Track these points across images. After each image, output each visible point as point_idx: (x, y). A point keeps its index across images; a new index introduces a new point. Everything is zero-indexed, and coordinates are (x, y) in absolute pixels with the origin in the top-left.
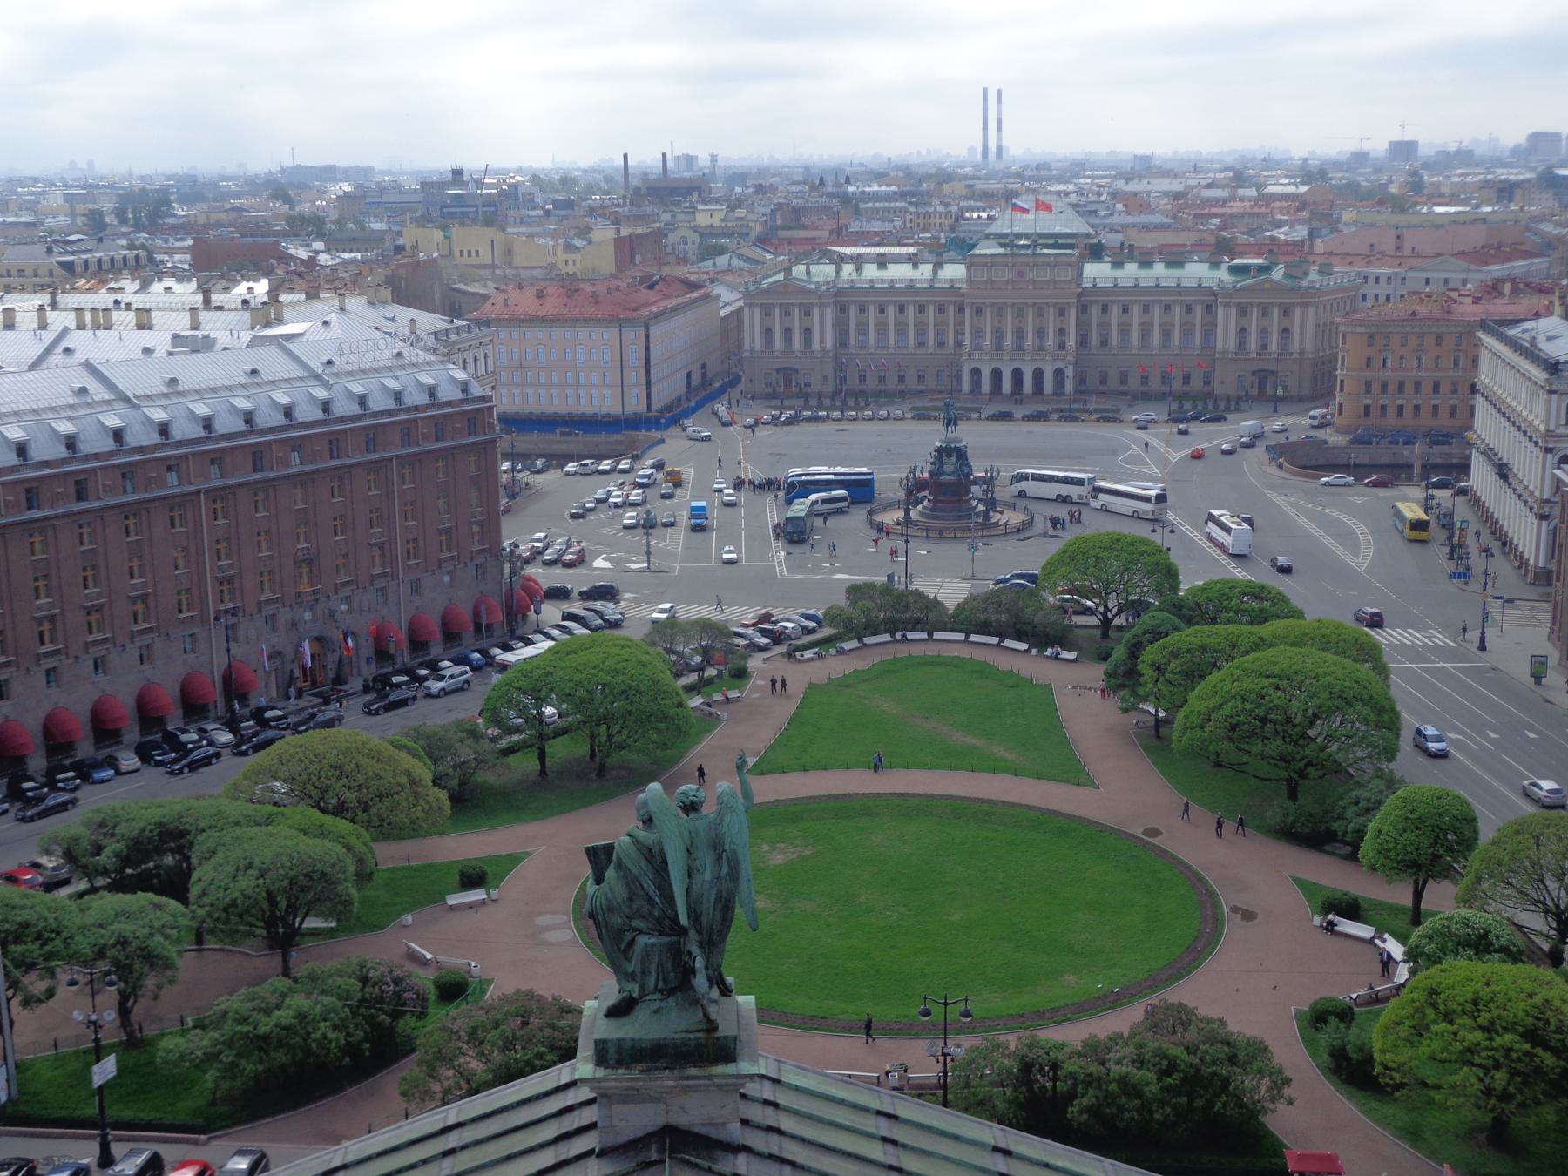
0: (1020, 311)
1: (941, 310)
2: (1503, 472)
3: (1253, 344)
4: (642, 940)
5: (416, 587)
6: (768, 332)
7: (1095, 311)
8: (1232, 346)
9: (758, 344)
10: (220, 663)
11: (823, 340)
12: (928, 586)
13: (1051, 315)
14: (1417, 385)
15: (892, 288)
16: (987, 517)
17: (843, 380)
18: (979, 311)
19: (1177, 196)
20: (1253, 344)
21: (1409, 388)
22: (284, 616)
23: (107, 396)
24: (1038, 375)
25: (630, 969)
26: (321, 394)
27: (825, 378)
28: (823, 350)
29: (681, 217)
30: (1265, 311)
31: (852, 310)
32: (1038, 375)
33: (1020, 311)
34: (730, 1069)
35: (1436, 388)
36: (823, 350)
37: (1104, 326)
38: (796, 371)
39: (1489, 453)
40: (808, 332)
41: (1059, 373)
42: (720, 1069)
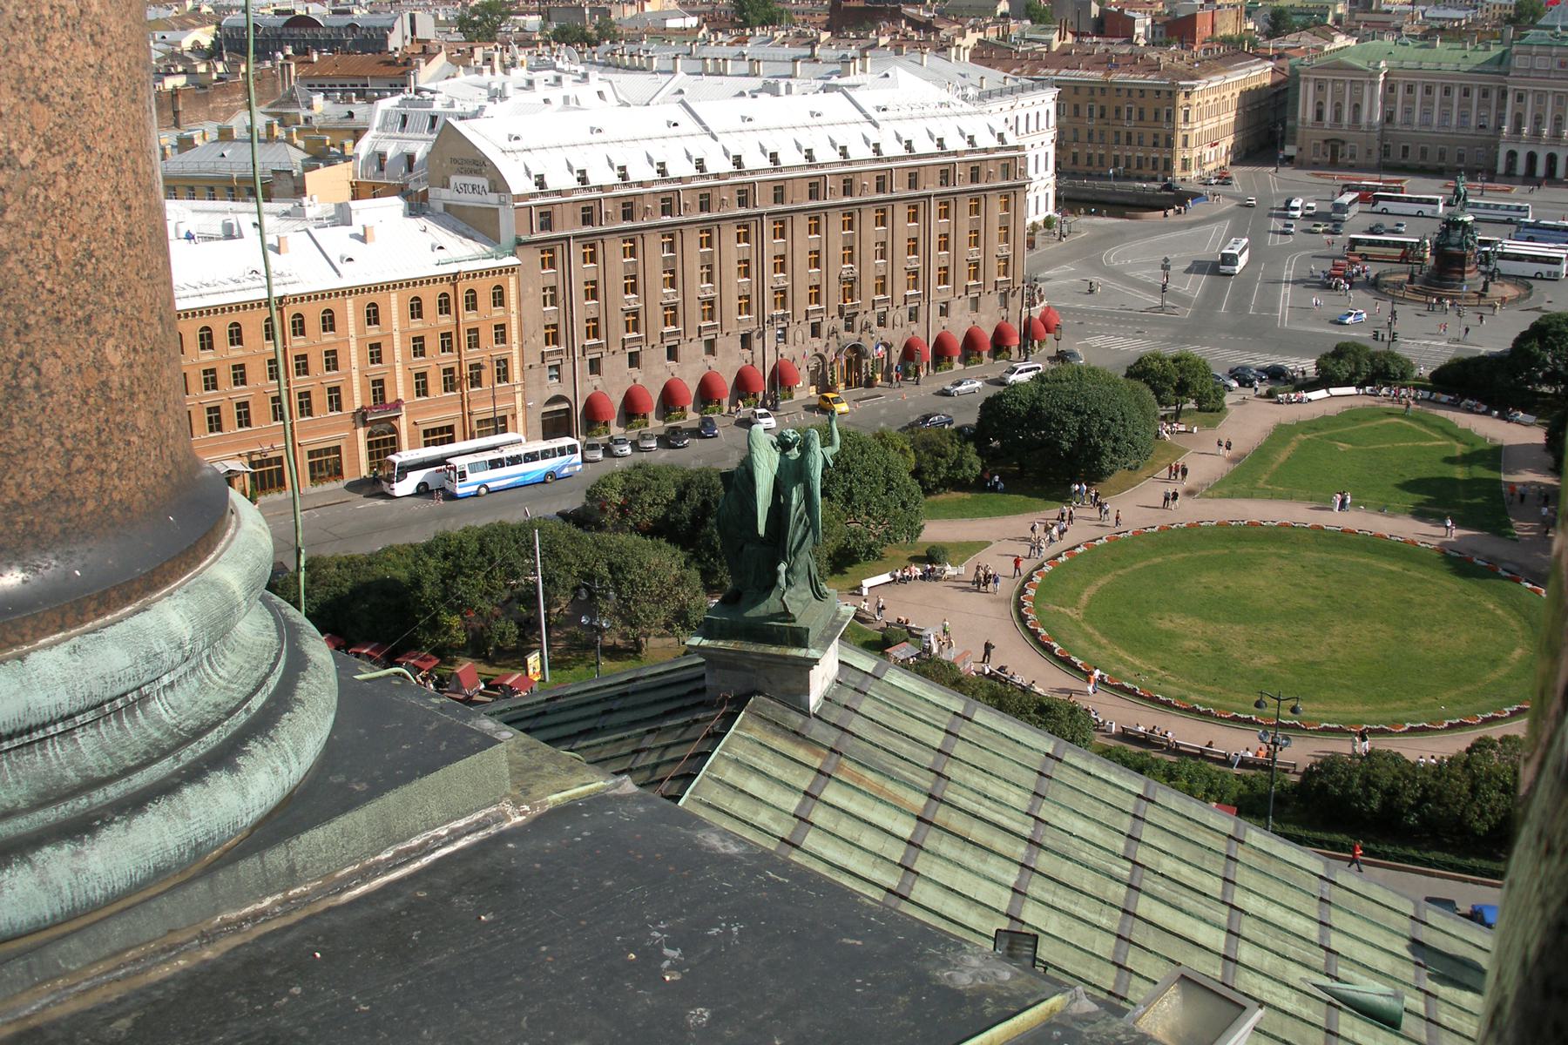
1: (1485, 94)
4: (748, 548)
9: (1310, 115)
11: (1370, 115)
12: (1406, 348)
16: (1485, 288)
17: (1387, 154)
18: (1520, 98)
23: (697, 128)
27: (1369, 152)
28: (1370, 125)
34: (801, 653)
36: (1370, 125)
38: (1343, 143)
40: (1357, 108)
42: (795, 652)
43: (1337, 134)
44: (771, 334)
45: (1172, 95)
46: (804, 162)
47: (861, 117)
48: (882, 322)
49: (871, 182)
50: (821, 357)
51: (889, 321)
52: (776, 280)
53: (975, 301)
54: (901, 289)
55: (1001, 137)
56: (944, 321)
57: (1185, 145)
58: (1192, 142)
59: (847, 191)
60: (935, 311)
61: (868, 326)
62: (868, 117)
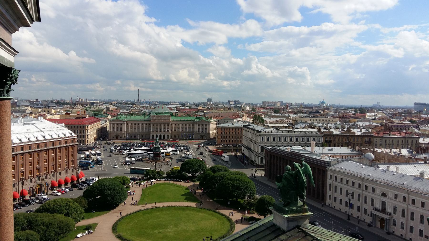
0: (161, 125)
1: (146, 124)
2: (250, 149)
3: (201, 130)
5: (60, 174)
6: (113, 128)
7: (173, 125)
8: (197, 131)
10: (20, 189)
13: (166, 125)
14: (229, 137)
15: (137, 121)
18: (153, 125)
19: (176, 108)
20: (201, 130)
21: (228, 137)
22: (33, 180)
24: (164, 136)
25: (288, 197)
26: (44, 135)
29: (88, 108)
30: (203, 125)
31: (129, 124)
32: (164, 136)
33: (161, 125)
35: (232, 138)
37: (175, 128)
39: (247, 147)
40: (121, 128)
41: (168, 135)
43: (117, 134)
44: (20, 183)
45: (84, 127)
46: (19, 142)
47: (39, 131)
48: (46, 178)
49: (43, 145)
50: (32, 188)
51: (48, 177)
52: (21, 170)
53: (67, 171)
54: (51, 170)
55: (71, 134)
56: (60, 176)
57: (88, 137)
58: (89, 137)
59: (53, 145)
60: (58, 174)
61: (43, 179)
62: (41, 130)
